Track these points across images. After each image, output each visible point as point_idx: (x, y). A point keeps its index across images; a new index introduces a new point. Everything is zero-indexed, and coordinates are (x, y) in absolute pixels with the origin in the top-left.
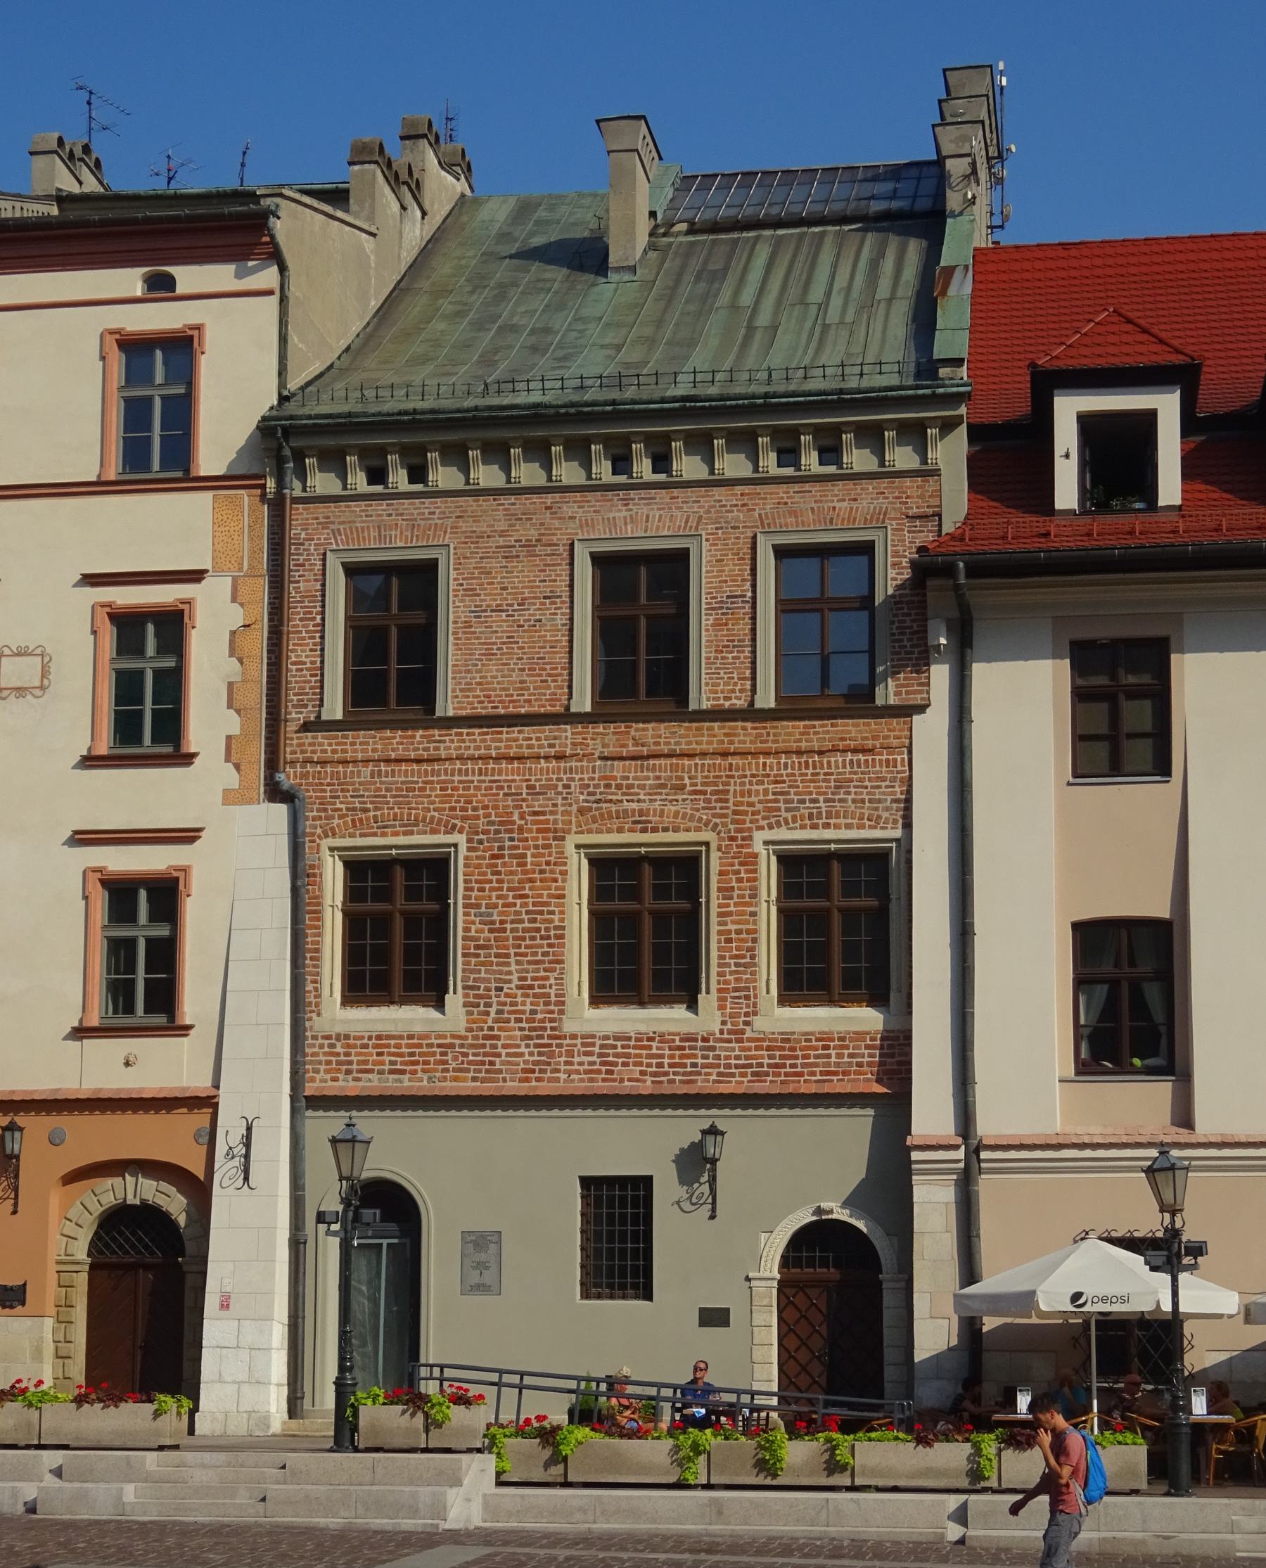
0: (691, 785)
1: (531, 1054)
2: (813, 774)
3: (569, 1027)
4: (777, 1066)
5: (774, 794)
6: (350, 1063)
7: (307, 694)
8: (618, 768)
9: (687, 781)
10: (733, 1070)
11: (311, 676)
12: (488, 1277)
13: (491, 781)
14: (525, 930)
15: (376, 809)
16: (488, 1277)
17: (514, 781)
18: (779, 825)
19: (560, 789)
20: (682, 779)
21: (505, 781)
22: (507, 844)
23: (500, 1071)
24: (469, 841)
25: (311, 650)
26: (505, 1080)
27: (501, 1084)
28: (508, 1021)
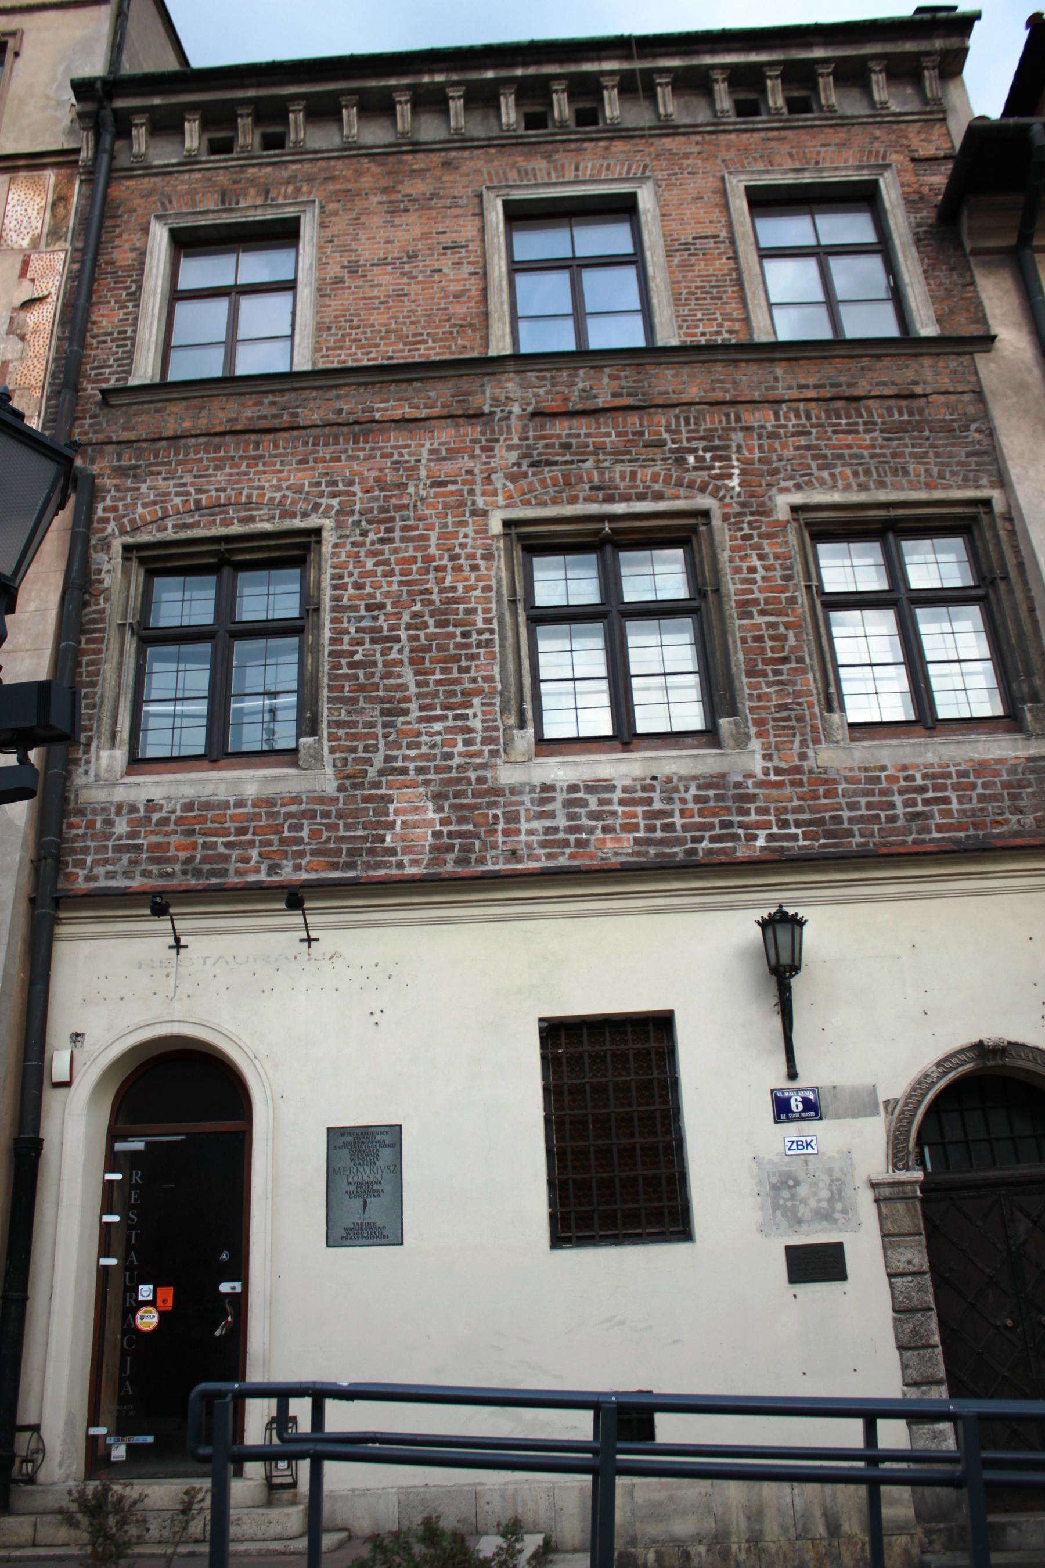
0: (674, 442)
1: (444, 822)
2: (847, 424)
3: (507, 776)
4: (861, 819)
5: (797, 448)
6: (138, 848)
7: (111, 366)
8: (560, 428)
9: (666, 436)
10: (793, 830)
11: (118, 346)
12: (376, 1211)
13: (373, 449)
14: (430, 637)
15: (199, 491)
16: (376, 1211)
17: (408, 446)
18: (809, 484)
19: (478, 452)
20: (659, 434)
21: (393, 447)
22: (399, 524)
23: (392, 852)
24: (339, 526)
25: (121, 320)
26: (400, 865)
27: (394, 872)
28: (404, 771)
